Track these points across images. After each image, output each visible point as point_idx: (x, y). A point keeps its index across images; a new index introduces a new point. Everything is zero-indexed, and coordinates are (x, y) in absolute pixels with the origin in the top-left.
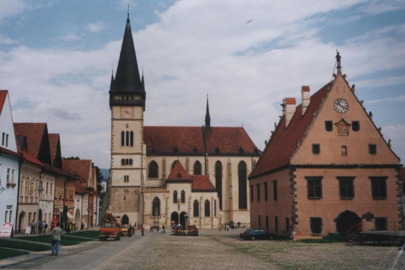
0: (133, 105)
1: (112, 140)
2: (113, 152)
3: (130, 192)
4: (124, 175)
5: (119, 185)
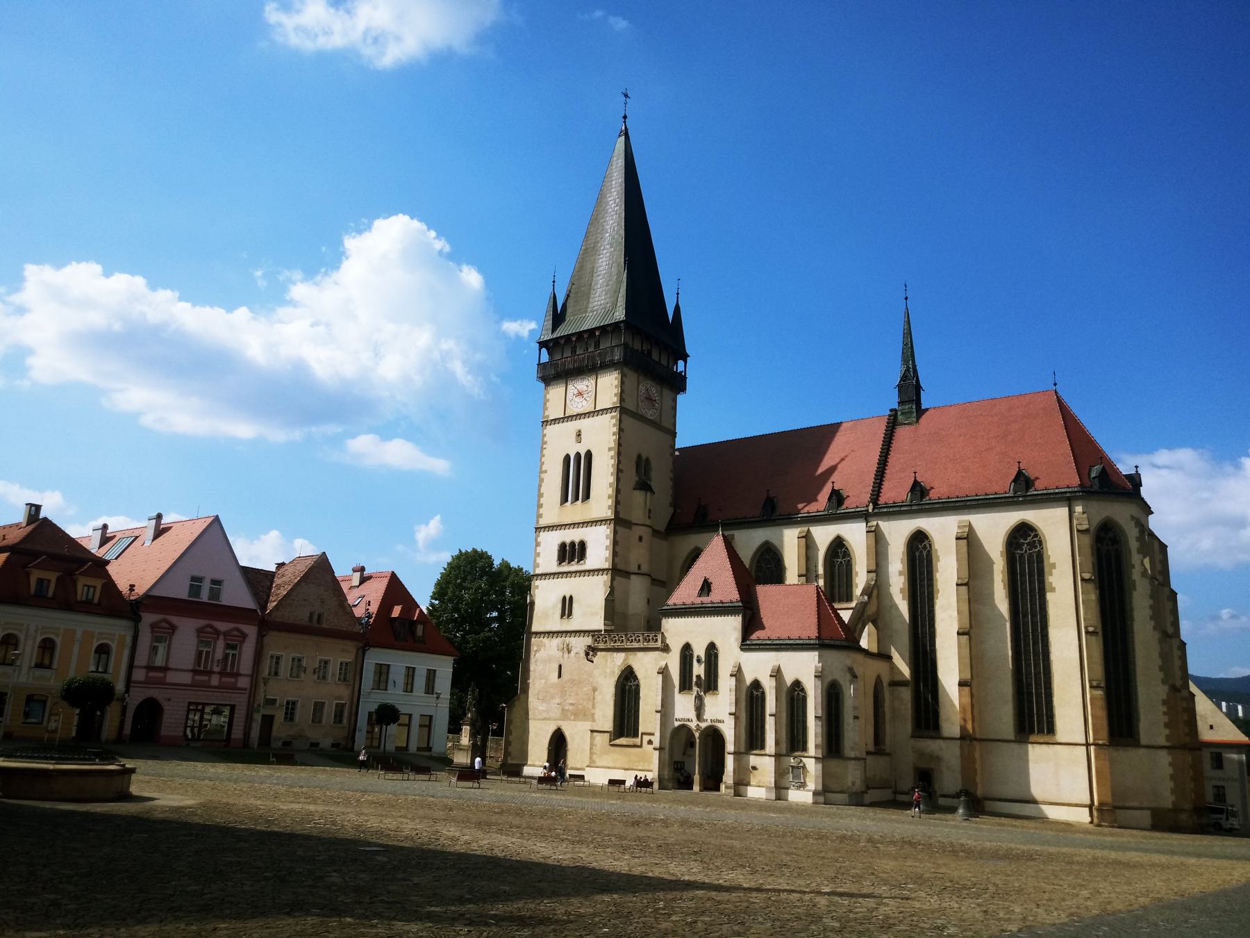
3: (573, 653)
5: (548, 628)
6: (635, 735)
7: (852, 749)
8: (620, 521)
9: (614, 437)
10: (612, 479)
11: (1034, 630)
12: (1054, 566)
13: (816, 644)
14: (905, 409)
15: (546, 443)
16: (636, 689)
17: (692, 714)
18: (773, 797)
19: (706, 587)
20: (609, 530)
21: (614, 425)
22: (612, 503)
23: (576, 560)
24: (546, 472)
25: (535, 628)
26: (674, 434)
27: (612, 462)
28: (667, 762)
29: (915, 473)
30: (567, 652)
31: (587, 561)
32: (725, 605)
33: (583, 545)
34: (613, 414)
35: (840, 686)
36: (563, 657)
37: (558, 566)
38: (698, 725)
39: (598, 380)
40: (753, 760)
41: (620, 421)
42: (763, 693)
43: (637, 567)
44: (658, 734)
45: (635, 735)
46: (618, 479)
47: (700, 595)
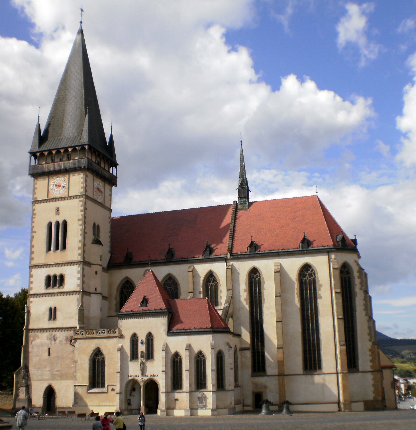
0: (66, 171)
1: (31, 241)
3: (57, 341)
4: (48, 308)
5: (41, 326)
6: (103, 386)
7: (230, 385)
8: (85, 263)
9: (82, 213)
10: (80, 238)
11: (312, 318)
12: (321, 286)
13: (211, 331)
14: (242, 202)
15: (35, 214)
17: (139, 373)
18: (189, 414)
19: (145, 301)
20: (79, 268)
21: (82, 206)
22: (81, 252)
23: (58, 286)
24: (35, 232)
25: (31, 326)
26: (110, 210)
27: (81, 227)
28: (124, 401)
29: (252, 237)
30: (53, 340)
31: (65, 286)
32: (157, 311)
33: (62, 277)
34: (81, 199)
35: (223, 352)
36: (51, 344)
37: (45, 289)
38: (142, 379)
39: (70, 177)
40: (177, 395)
41: (85, 203)
42: (181, 359)
43: (94, 289)
44: (118, 385)
45: (103, 386)
46: (84, 238)
47: (141, 306)
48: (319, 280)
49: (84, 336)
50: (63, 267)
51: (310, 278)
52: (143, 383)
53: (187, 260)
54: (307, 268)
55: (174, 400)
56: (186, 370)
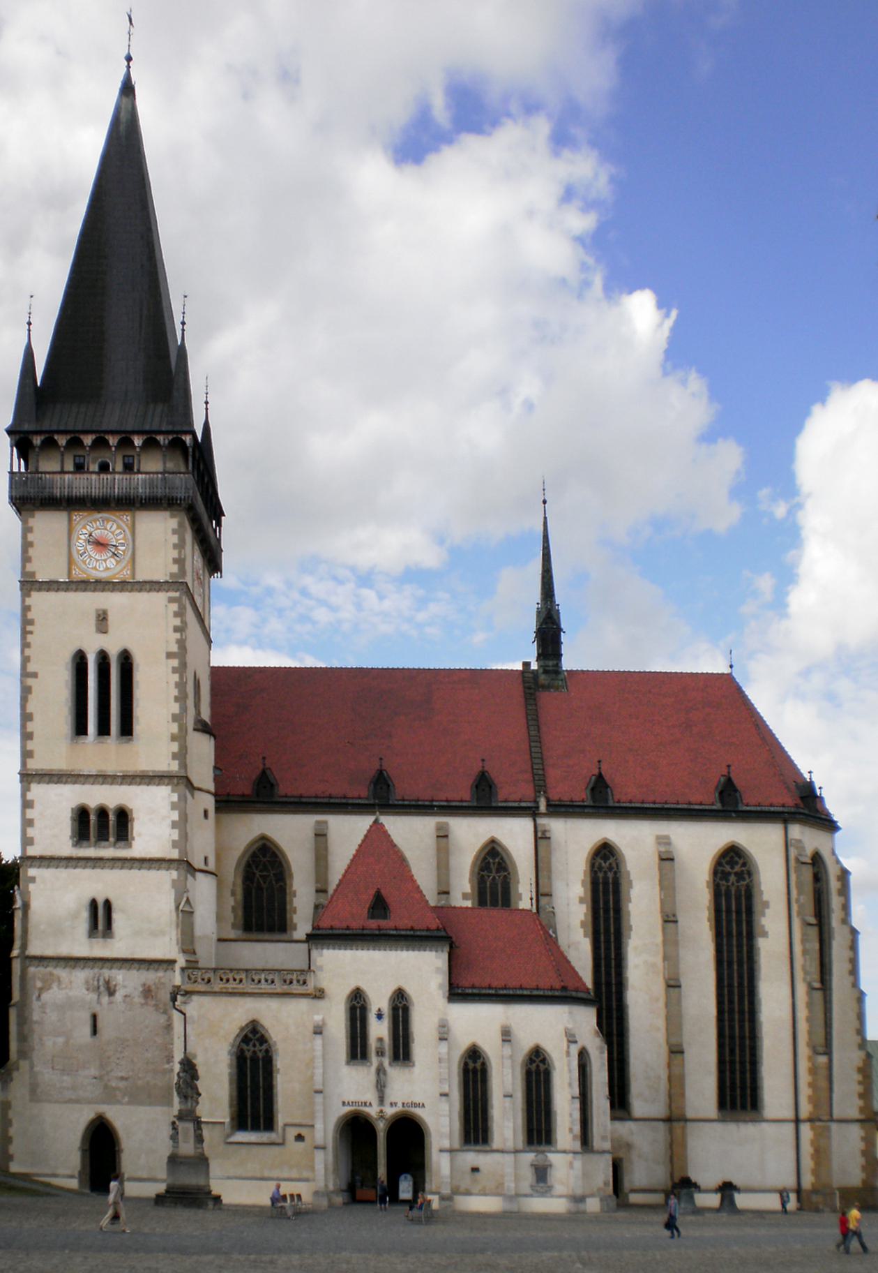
2: (34, 765)
7: (604, 1138)
12: (766, 905)
16: (263, 1058)
17: (370, 1096)
24: (35, 675)
33: (123, 816)
38: (381, 1111)
48: (762, 891)
49: (213, 988)
50: (125, 788)
51: (739, 884)
52: (384, 1125)
53: (432, 807)
54: (732, 857)
55: (468, 1169)
56: (506, 1094)
